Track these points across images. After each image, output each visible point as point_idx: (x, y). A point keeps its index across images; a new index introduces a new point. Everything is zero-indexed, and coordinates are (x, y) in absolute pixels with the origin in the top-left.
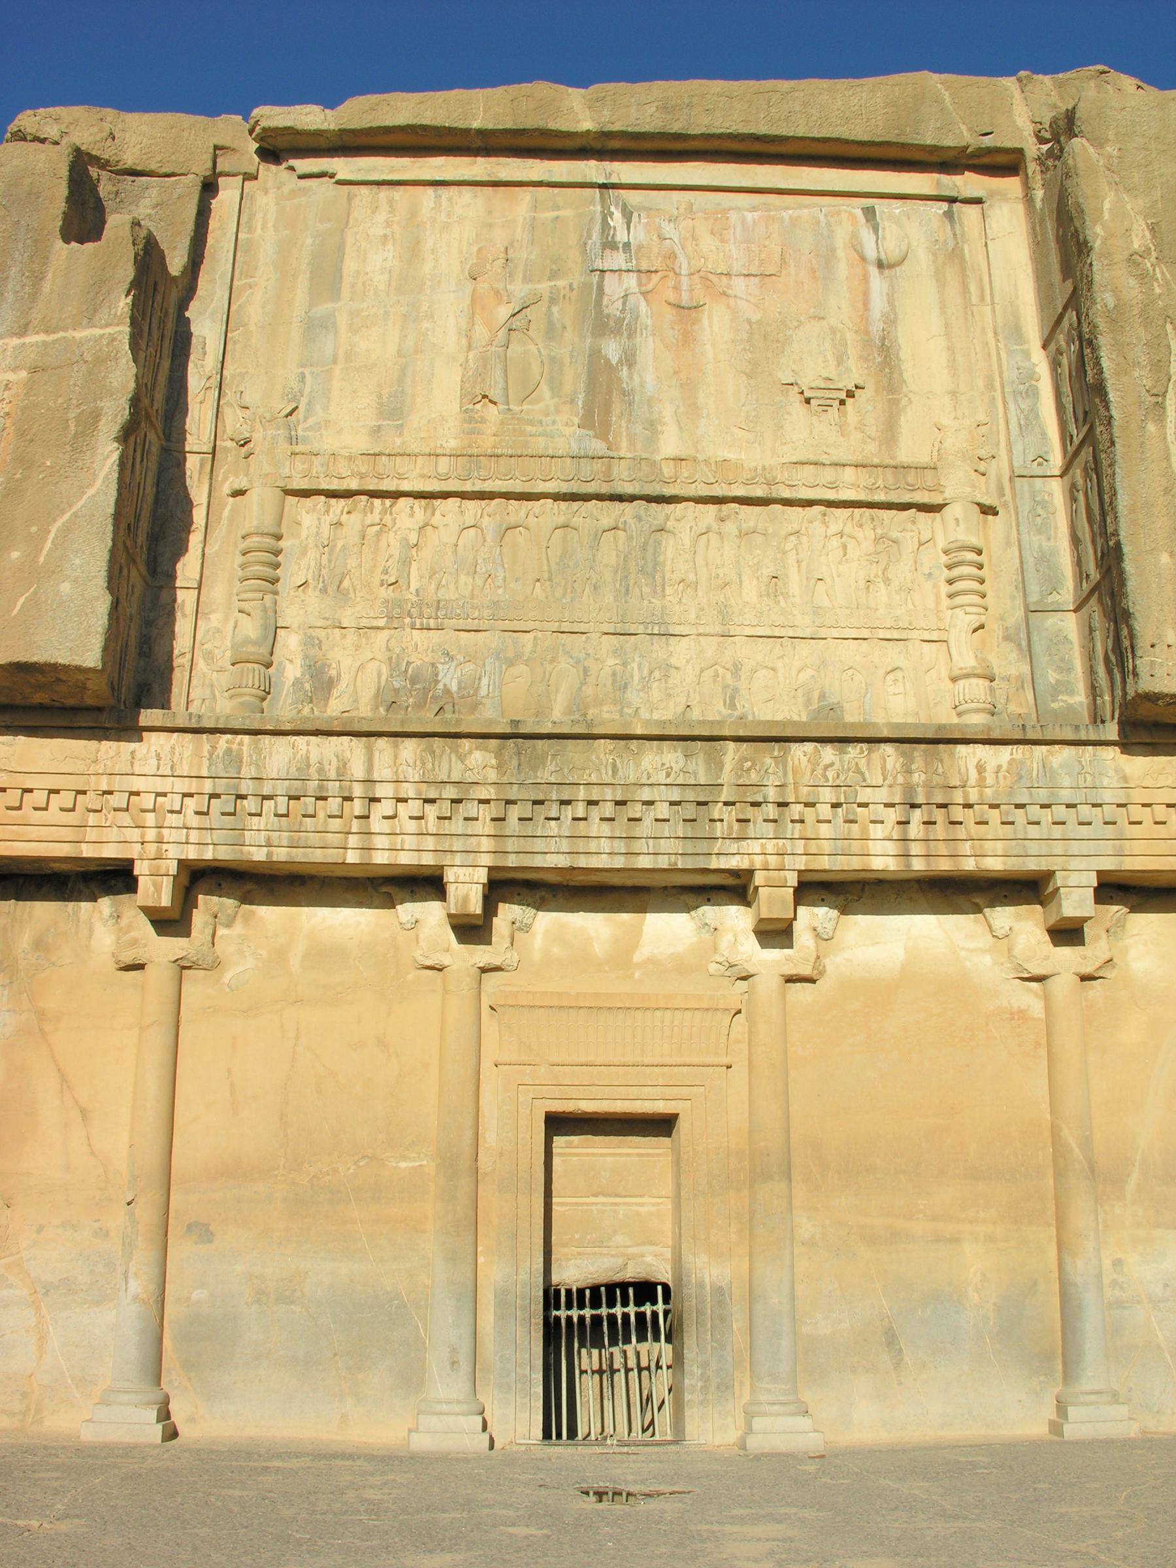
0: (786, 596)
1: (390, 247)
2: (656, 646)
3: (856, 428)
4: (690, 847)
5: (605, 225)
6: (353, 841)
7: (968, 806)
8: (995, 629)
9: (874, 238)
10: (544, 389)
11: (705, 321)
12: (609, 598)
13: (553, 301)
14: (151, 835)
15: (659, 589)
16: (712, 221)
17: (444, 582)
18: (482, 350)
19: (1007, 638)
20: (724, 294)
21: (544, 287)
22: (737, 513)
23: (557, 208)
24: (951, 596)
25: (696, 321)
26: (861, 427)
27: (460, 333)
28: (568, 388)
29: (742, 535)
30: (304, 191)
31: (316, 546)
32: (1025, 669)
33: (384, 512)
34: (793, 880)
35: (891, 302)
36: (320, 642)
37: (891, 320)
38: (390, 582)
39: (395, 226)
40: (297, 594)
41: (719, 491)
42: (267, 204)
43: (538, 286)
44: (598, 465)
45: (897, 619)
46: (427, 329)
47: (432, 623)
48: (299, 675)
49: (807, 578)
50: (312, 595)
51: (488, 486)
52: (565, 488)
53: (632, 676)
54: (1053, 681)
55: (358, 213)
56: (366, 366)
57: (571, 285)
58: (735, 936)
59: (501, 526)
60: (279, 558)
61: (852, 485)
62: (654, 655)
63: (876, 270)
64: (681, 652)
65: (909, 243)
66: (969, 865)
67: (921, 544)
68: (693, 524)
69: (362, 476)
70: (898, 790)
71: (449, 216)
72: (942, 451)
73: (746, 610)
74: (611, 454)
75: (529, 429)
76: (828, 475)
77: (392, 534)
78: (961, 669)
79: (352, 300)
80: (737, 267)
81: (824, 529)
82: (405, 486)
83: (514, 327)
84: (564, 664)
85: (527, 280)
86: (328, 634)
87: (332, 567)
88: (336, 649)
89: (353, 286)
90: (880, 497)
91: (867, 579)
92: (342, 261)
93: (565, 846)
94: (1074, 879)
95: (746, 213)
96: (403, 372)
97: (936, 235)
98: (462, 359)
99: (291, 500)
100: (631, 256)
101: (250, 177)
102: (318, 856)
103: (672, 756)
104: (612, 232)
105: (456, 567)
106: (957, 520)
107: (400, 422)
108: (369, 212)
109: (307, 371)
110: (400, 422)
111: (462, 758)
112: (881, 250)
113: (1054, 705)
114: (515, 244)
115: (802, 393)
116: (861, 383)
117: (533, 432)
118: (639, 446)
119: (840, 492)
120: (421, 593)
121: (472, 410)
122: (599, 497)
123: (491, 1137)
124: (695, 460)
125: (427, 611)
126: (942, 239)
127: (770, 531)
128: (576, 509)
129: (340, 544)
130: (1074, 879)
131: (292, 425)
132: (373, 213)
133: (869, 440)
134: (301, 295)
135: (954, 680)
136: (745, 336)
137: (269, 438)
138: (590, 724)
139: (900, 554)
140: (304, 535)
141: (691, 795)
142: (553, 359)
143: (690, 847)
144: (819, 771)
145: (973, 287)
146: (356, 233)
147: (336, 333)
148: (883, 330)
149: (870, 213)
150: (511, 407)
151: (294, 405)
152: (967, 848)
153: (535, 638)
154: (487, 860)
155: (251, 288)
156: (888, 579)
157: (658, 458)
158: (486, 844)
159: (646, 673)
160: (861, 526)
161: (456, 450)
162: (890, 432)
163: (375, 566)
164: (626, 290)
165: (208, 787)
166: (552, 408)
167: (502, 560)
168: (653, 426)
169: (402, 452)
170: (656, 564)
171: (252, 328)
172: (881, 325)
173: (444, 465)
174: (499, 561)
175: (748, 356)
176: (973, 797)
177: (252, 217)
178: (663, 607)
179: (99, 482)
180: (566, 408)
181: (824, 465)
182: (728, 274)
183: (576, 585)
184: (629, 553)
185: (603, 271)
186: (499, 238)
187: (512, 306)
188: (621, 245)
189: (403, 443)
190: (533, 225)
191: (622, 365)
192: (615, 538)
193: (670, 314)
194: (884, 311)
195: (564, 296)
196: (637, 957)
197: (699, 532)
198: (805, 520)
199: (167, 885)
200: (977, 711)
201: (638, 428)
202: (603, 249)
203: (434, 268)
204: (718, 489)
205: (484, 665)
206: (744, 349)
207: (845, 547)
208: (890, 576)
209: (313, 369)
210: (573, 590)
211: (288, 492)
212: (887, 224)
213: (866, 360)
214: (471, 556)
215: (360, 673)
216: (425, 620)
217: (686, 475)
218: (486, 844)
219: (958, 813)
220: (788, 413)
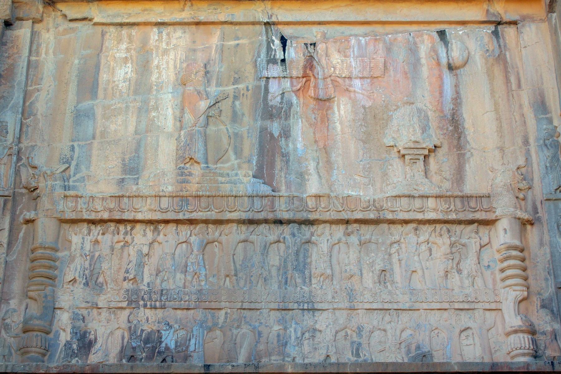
0: (393, 282)
1: (129, 65)
2: (306, 317)
3: (436, 173)
5: (269, 49)
9: (444, 51)
10: (231, 153)
11: (336, 109)
12: (275, 286)
13: (236, 98)
15: (307, 280)
16: (338, 44)
17: (166, 278)
18: (189, 129)
20: (347, 90)
22: (358, 230)
23: (237, 38)
24: (503, 280)
25: (329, 108)
26: (439, 172)
27: (175, 119)
28: (246, 152)
29: (361, 244)
31: (81, 255)
33: (126, 233)
36: (84, 318)
38: (130, 278)
39: (132, 52)
40: (68, 286)
41: (345, 216)
42: (49, 38)
43: (226, 88)
44: (265, 201)
46: (154, 117)
48: (69, 339)
49: (406, 270)
51: (194, 216)
52: (244, 216)
53: (290, 337)
55: (107, 44)
56: (114, 140)
57: (247, 88)
59: (203, 241)
60: (57, 264)
61: (434, 209)
62: (305, 323)
63: (448, 71)
65: (469, 53)
67: (481, 247)
68: (329, 238)
69: (111, 211)
71: (167, 44)
72: (494, 186)
73: (365, 293)
74: (273, 193)
75: (220, 179)
76: (418, 203)
77: (131, 247)
78: (512, 327)
79: (105, 98)
80: (355, 73)
81: (416, 238)
82: (140, 217)
83: (210, 114)
84: (245, 329)
85: (219, 84)
86: (89, 312)
87: (92, 269)
88: (94, 322)
89: (105, 90)
90: (453, 216)
91: (446, 270)
92: (98, 74)
95: (361, 38)
97: (487, 46)
98: (176, 135)
99: (66, 226)
100: (286, 68)
104: (273, 53)
105: (173, 268)
106: (505, 230)
107: (136, 176)
108: (115, 42)
109: (76, 144)
110: (136, 176)
112: (450, 58)
114: (211, 62)
115: (399, 152)
116: (438, 143)
117: (223, 181)
118: (293, 189)
119: (426, 214)
120: (151, 285)
121: (183, 168)
122: (266, 221)
124: (329, 196)
125: (154, 297)
126: (491, 49)
127: (380, 241)
128: (252, 229)
129: (97, 254)
131: (65, 179)
132: (118, 43)
133: (445, 181)
135: (508, 334)
136: (361, 116)
137: (49, 187)
139: (468, 254)
140: (73, 249)
142: (236, 135)
145: (513, 79)
146: (107, 56)
147: (94, 120)
148: (453, 109)
149: (442, 34)
150: (210, 165)
151: (67, 165)
153: (226, 313)
155: (38, 91)
156: (460, 270)
157: (305, 196)
159: (299, 334)
160: (441, 235)
161: (172, 192)
164: (283, 90)
166: (236, 166)
167: (204, 263)
168: (302, 176)
169: (137, 194)
170: (305, 264)
171: (39, 116)
172: (452, 106)
174: (202, 264)
177: (39, 46)
178: (311, 292)
180: (245, 166)
181: (414, 197)
182: (350, 78)
183: (252, 279)
184: (287, 257)
185: (268, 78)
186: (201, 57)
187: (209, 101)
188: (279, 61)
189: (138, 189)
190: (221, 50)
191: (281, 137)
192: (278, 249)
194: (454, 97)
195: (243, 95)
197: (333, 243)
198: (403, 234)
201: (293, 177)
202: (268, 64)
203: (158, 78)
204: (345, 214)
205: (192, 331)
206: (361, 125)
207: (430, 250)
208: (461, 268)
209: (80, 143)
210: (251, 282)
211: (63, 221)
212: (454, 41)
213: (442, 129)
214: (184, 261)
215: (110, 338)
216: (153, 303)
217: (323, 206)
220: (391, 165)
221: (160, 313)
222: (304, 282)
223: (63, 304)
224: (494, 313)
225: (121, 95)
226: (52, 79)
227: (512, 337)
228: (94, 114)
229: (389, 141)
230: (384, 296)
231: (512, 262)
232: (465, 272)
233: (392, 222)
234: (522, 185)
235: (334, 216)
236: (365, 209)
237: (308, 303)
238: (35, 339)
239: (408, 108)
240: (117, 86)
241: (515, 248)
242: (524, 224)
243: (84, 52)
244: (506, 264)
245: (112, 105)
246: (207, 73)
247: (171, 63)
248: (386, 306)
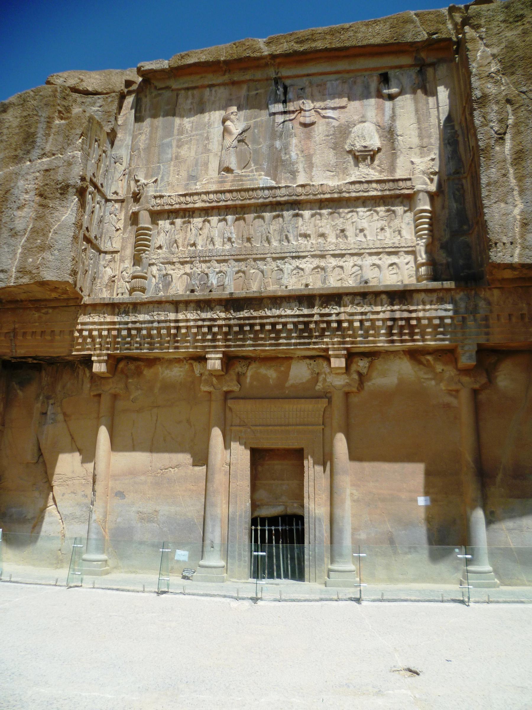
8: (437, 244)
11: (316, 129)
13: (255, 127)
19: (442, 247)
21: (251, 122)
23: (257, 89)
30: (160, 95)
32: (450, 260)
45: (394, 243)
47: (207, 258)
54: (461, 263)
58: (326, 375)
71: (215, 97)
74: (277, 186)
79: (178, 135)
98: (219, 154)
105: (216, 235)
113: (462, 274)
115: (355, 154)
132: (186, 100)
159: (290, 271)
163: (186, 238)
166: (254, 171)
168: (294, 174)
173: (211, 196)
175: (333, 141)
179: (69, 212)
203: (209, 119)
206: (332, 138)
220: (350, 163)
221: (208, 264)
222: (294, 239)
225: (187, 132)
226: (148, 126)
228: (171, 145)
230: (342, 246)
237: (296, 252)
240: (185, 126)
243: (166, 108)
245: (182, 139)
248: (343, 252)
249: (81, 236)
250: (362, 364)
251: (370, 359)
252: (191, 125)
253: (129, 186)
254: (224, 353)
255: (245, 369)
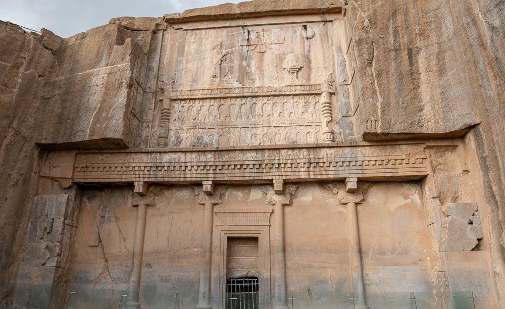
4: (258, 174)
6: (182, 176)
7: (324, 163)
13: (231, 53)
14: (137, 176)
19: (337, 123)
24: (323, 114)
29: (273, 104)
34: (282, 181)
35: (310, 47)
37: (309, 51)
47: (203, 127)
50: (177, 122)
51: (216, 96)
64: (259, 131)
66: (325, 177)
67: (316, 103)
69: (188, 95)
70: (307, 160)
76: (294, 88)
82: (197, 97)
90: (306, 92)
93: (229, 175)
94: (351, 179)
96: (197, 71)
99: (173, 102)
101: (164, 30)
102: (174, 180)
103: (254, 154)
111: (206, 156)
122: (240, 97)
123: (215, 243)
130: (351, 179)
134: (175, 56)
135: (324, 134)
138: (234, 147)
141: (257, 162)
143: (258, 174)
144: (288, 156)
145: (330, 42)
152: (324, 173)
154: (212, 179)
158: (211, 175)
159: (251, 136)
162: (309, 79)
165: (150, 165)
168: (253, 80)
176: (325, 160)
193: (257, 54)
196: (249, 201)
199: (141, 187)
200: (329, 141)
218: (211, 175)
219: (321, 165)
221: (204, 130)
223: (172, 128)
224: (319, 127)
227: (325, 135)
229: (284, 66)
231: (326, 108)
232: (309, 113)
233: (284, 95)
234: (332, 80)
235: (264, 94)
236: (275, 91)
238: (162, 140)
239: (292, 54)
241: (328, 103)
242: (332, 94)
243: (180, 40)
244: (324, 109)
246: (221, 45)
247: (209, 42)
249: (129, 112)
250: (292, 189)
251: (296, 186)
252: (194, 51)
253: (157, 84)
254: (213, 181)
255: (224, 191)
